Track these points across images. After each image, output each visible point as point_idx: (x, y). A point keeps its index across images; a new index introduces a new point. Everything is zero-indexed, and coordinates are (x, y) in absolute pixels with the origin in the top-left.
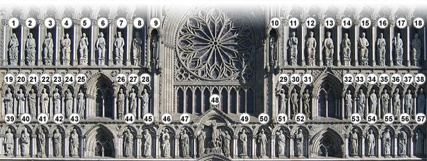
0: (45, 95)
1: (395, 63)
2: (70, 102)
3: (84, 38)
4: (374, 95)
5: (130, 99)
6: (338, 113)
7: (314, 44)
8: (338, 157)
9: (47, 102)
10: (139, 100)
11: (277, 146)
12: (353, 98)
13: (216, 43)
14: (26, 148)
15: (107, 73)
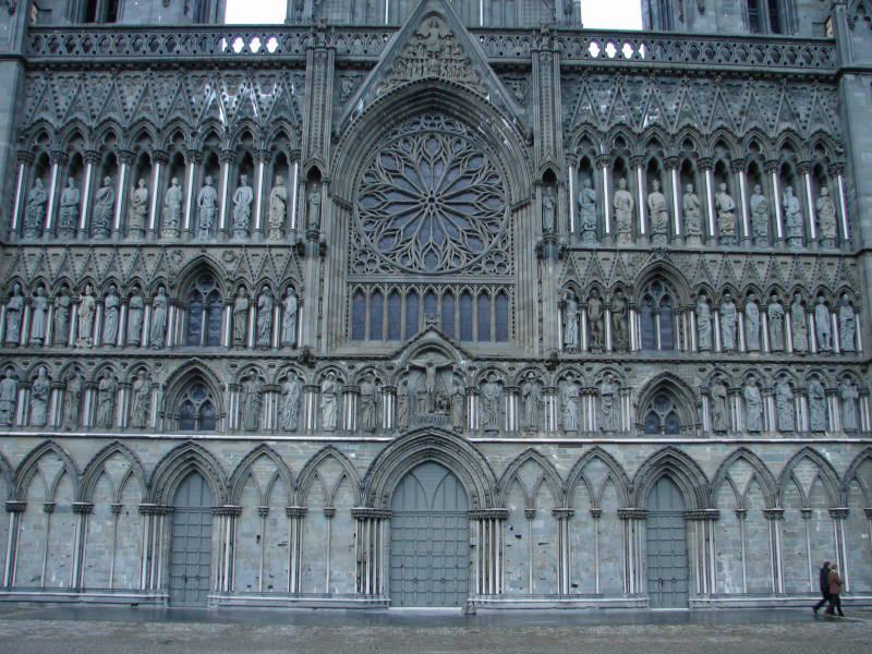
0: (88, 300)
1: (787, 240)
2: (135, 316)
3: (174, 187)
4: (754, 306)
5: (258, 309)
6: (682, 342)
7: (628, 203)
8: (689, 436)
9: (91, 314)
10: (277, 310)
11: (562, 408)
12: (712, 311)
13: (432, 200)
14: (38, 410)
15: (216, 255)
